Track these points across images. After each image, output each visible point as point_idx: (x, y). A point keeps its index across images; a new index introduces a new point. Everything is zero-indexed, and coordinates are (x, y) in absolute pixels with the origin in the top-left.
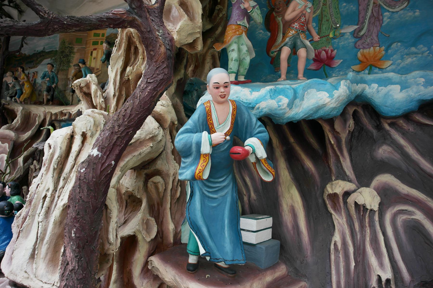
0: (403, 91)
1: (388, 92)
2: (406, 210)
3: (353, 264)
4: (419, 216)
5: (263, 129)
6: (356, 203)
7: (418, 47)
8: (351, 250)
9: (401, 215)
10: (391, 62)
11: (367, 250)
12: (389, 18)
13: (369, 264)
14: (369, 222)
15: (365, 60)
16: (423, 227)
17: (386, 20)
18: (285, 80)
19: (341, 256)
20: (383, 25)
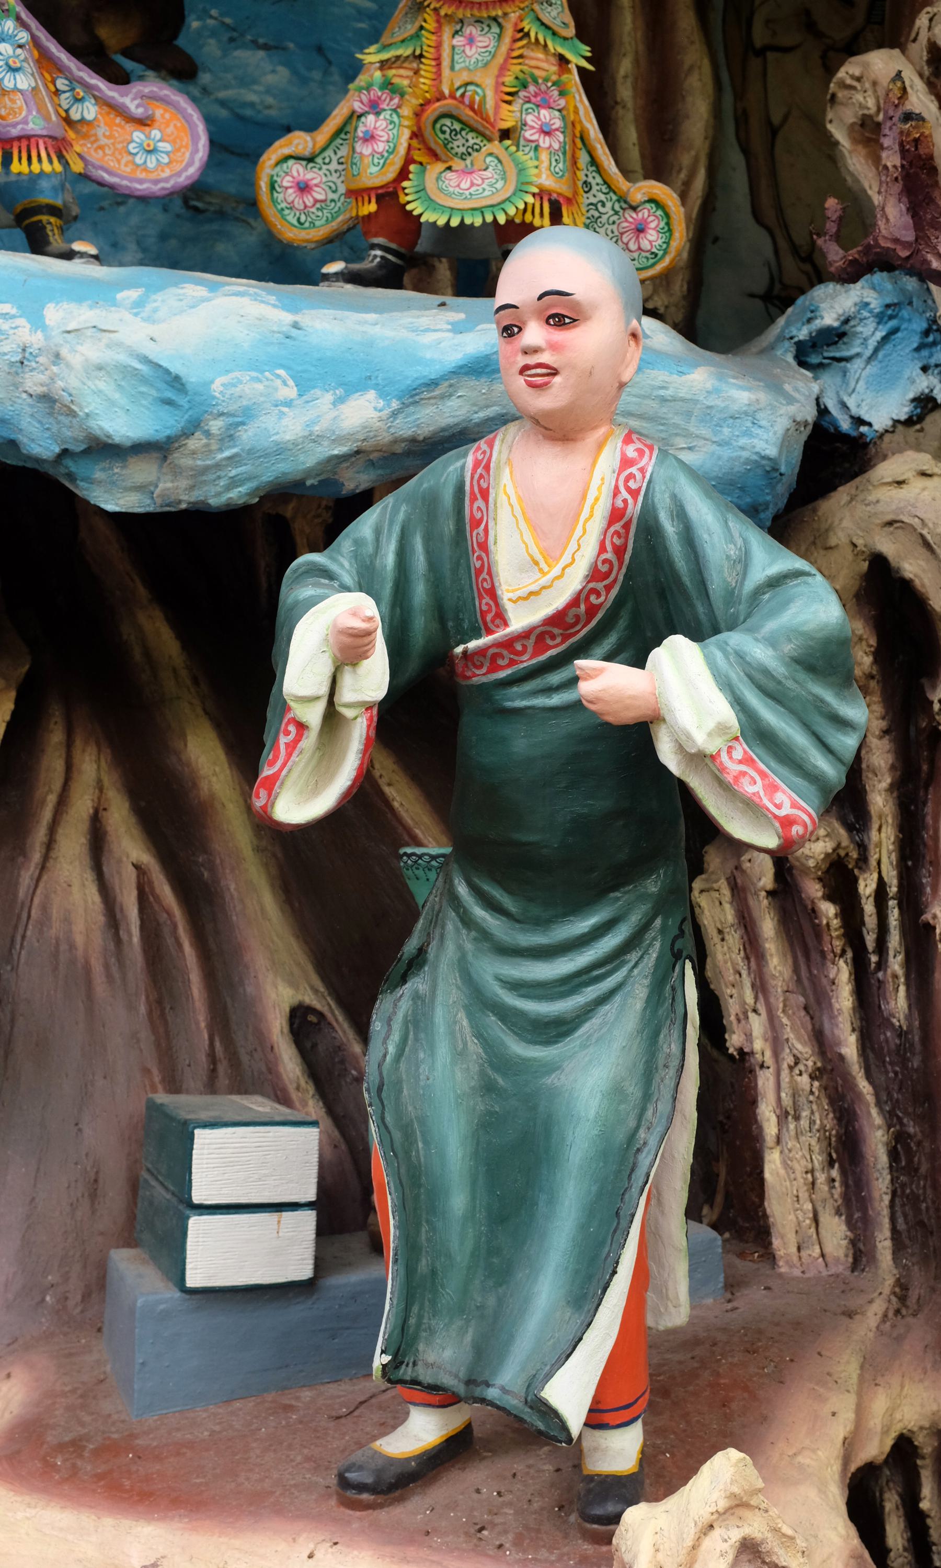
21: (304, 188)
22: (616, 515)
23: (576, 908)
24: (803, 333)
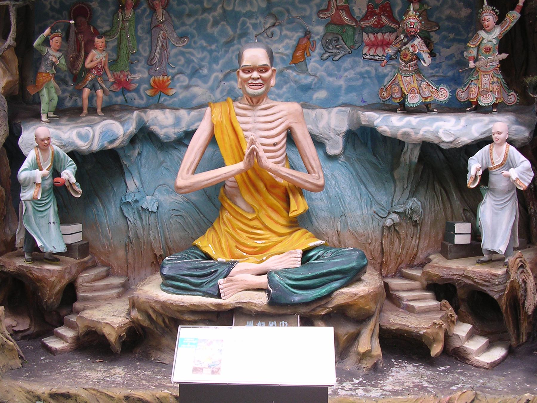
5: (73, 162)
18: (87, 115)
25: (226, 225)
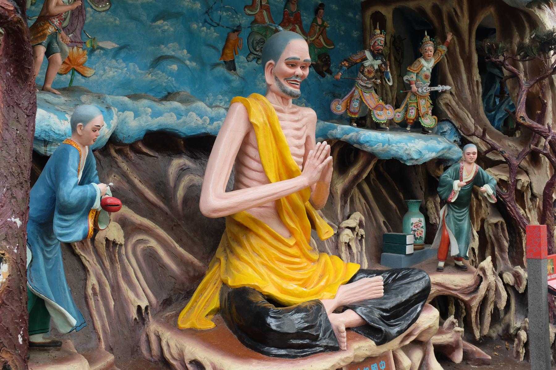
0: (136, 119)
1: (125, 118)
2: (142, 239)
3: (112, 303)
4: (153, 243)
6: (107, 240)
7: (118, 61)
8: (108, 290)
9: (140, 245)
10: (93, 72)
11: (122, 286)
12: (92, 16)
13: (125, 298)
14: (118, 257)
15: (68, 62)
16: (156, 252)
17: (89, 19)
19: (99, 299)
20: (86, 22)
21: (399, 116)
22: (476, 172)
23: (464, 208)
24: (441, 131)
25: (259, 255)
